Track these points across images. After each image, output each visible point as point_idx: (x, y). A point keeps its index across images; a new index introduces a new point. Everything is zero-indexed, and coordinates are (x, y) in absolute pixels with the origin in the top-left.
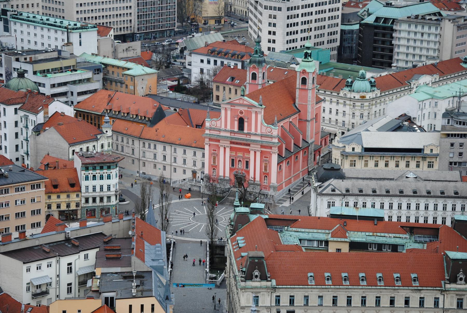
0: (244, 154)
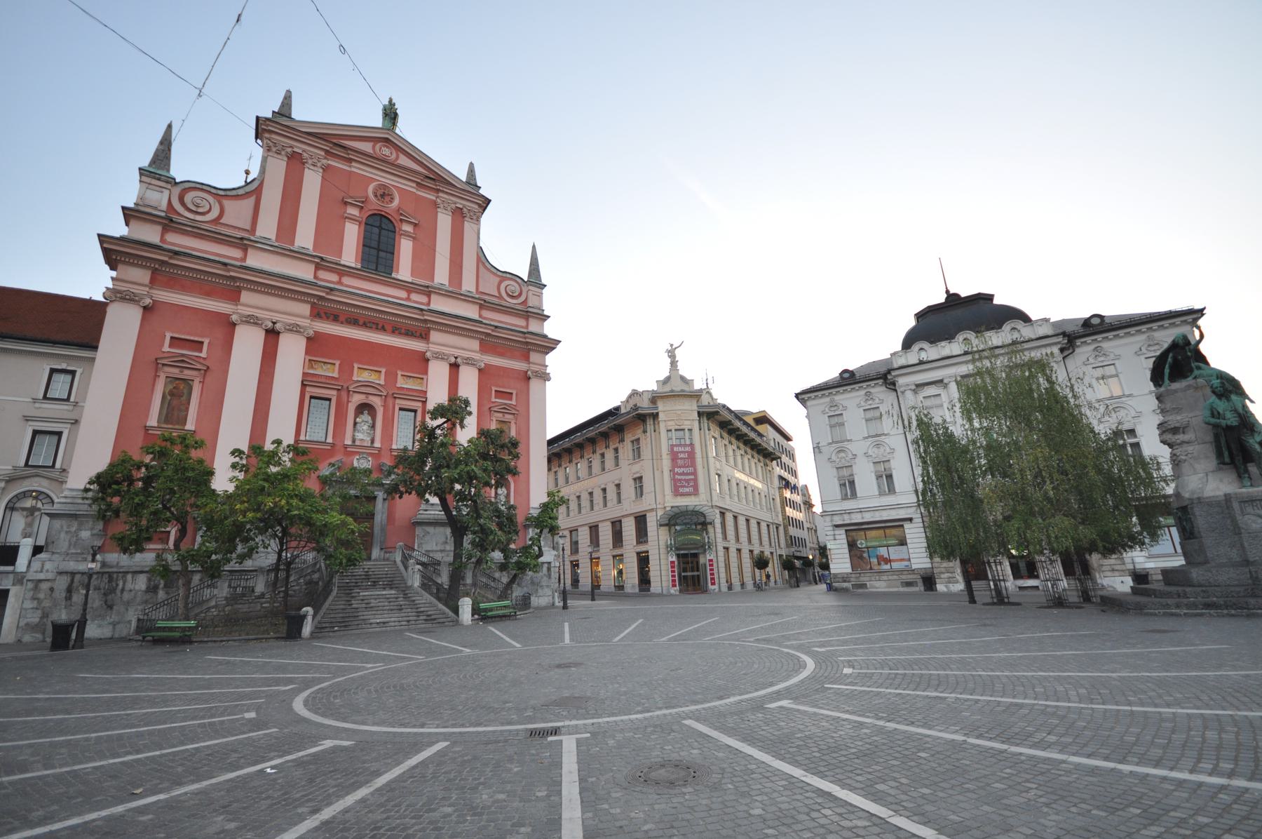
0: (391, 377)
